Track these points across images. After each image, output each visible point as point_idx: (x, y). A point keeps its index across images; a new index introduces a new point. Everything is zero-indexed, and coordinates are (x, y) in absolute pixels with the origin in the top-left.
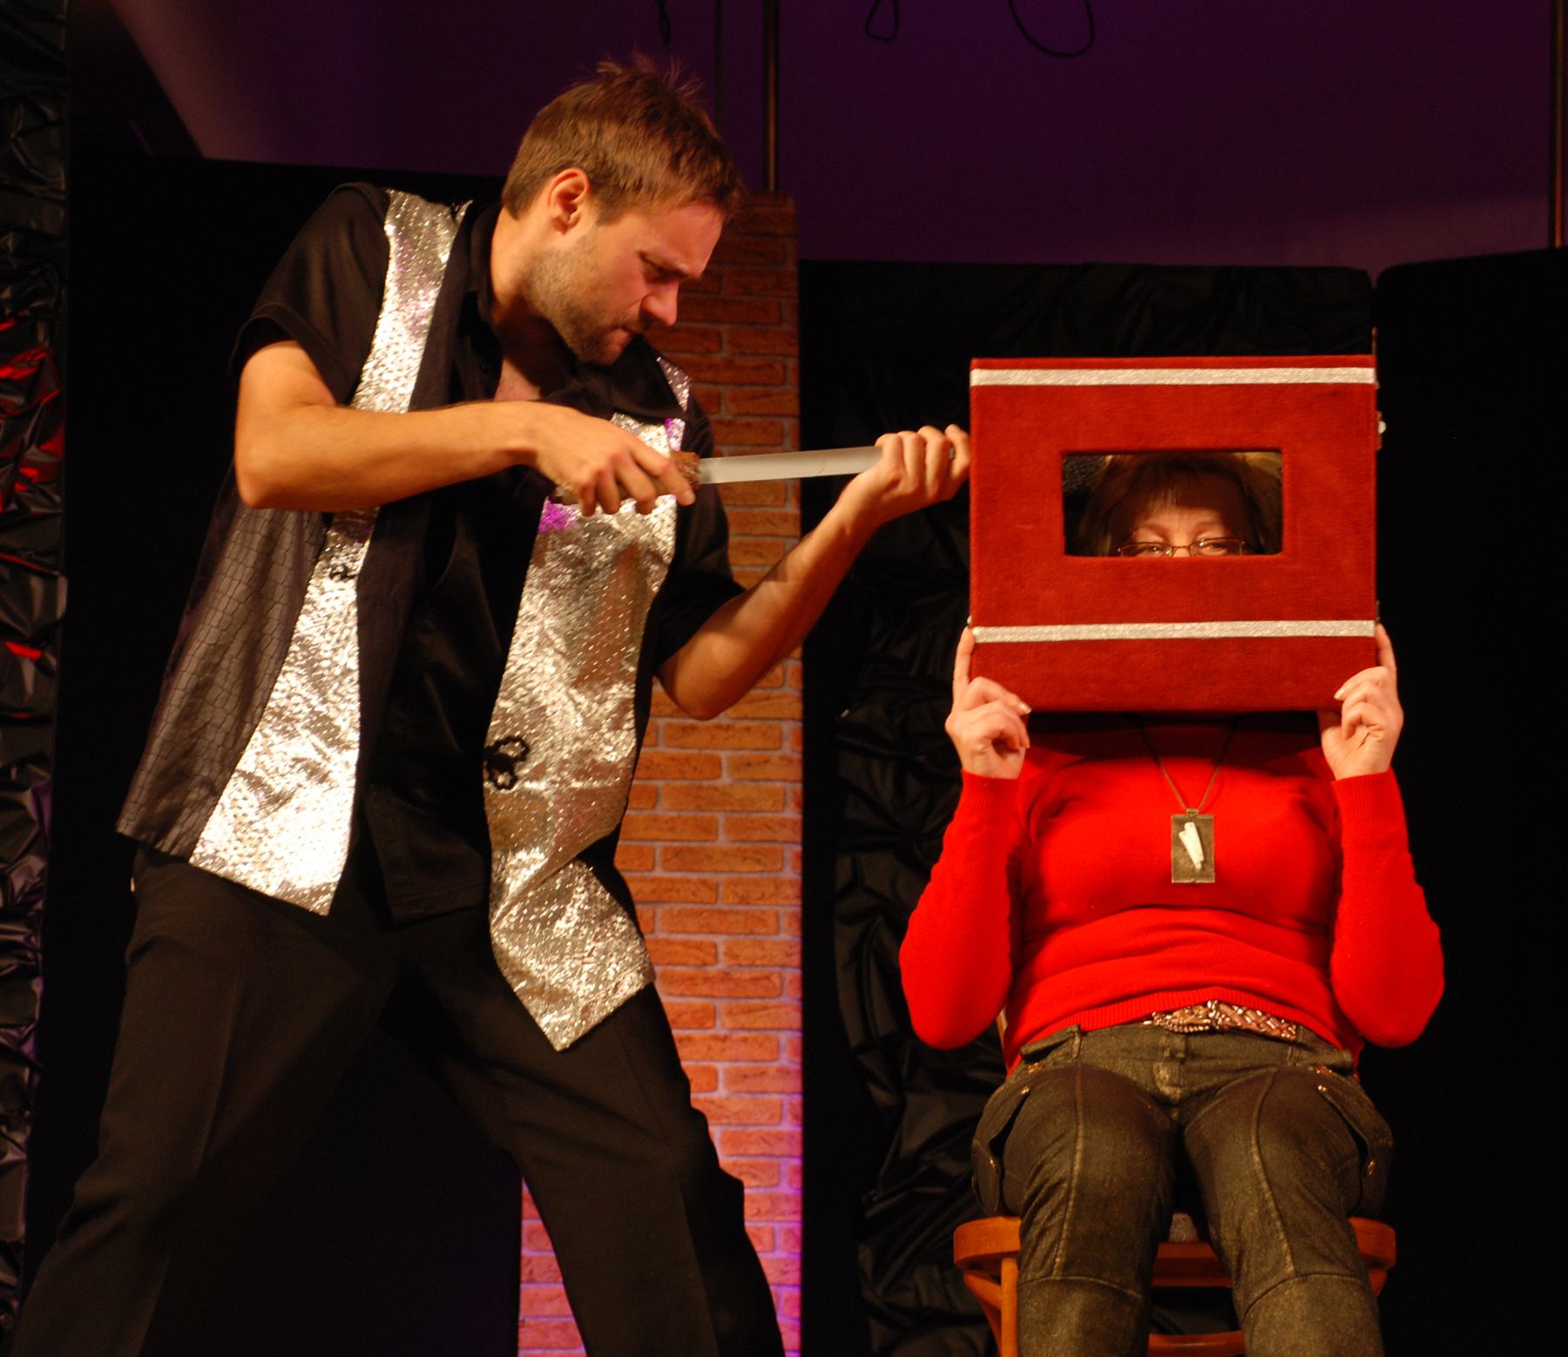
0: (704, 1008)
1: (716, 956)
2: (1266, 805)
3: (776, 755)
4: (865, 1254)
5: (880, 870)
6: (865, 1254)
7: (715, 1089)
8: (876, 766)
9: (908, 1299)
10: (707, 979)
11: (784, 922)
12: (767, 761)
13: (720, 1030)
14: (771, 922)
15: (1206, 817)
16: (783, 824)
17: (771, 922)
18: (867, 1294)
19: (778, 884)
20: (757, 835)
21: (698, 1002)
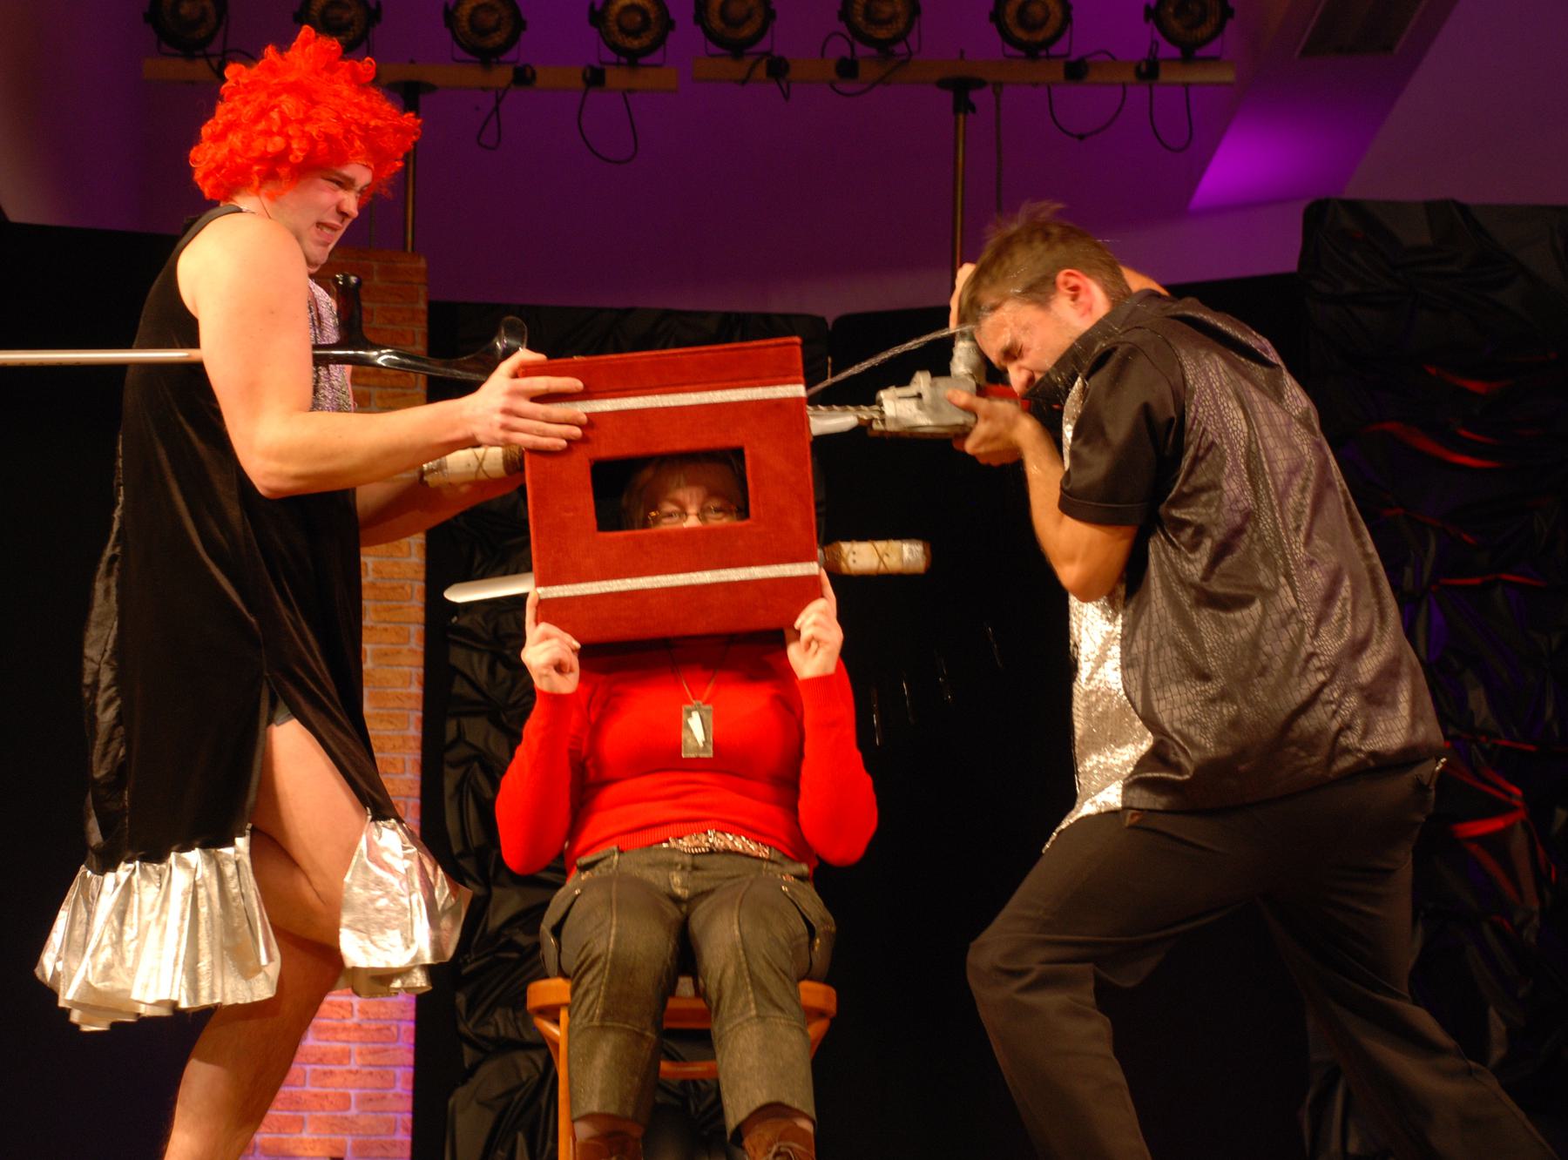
0: (343, 1051)
1: (352, 1012)
2: (750, 702)
3: (405, 648)
4: (461, 999)
5: (478, 731)
6: (461, 999)
7: (348, 1108)
8: (475, 657)
9: (490, 1031)
10: (345, 1029)
11: (409, 765)
12: (399, 652)
13: (353, 1066)
14: (399, 765)
15: (709, 707)
16: (409, 696)
17: (399, 765)
18: (462, 1028)
19: (405, 739)
20: (391, 704)
21: (338, 1046)
